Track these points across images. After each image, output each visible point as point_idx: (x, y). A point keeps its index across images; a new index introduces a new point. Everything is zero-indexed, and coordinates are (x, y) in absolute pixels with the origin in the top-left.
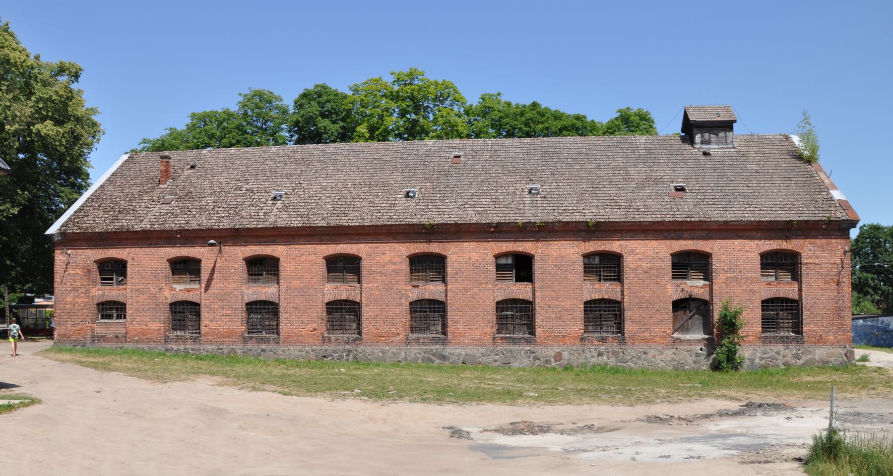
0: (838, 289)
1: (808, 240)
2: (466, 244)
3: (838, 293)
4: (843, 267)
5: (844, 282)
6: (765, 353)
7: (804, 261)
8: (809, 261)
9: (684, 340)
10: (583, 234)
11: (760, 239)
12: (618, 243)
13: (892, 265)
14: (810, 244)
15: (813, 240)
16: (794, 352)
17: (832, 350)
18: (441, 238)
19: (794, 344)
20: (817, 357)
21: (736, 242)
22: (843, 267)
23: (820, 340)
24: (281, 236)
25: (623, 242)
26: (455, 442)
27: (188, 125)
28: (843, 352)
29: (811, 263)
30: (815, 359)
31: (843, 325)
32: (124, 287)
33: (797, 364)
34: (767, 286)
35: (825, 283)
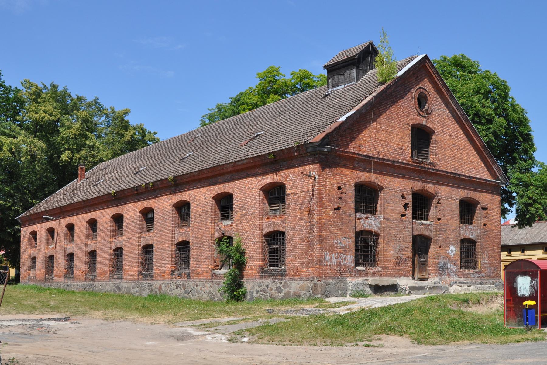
0: (309, 219)
1: (290, 170)
2: (130, 205)
3: (310, 222)
4: (313, 195)
5: (314, 210)
6: (260, 286)
7: (288, 191)
8: (291, 191)
9: (218, 274)
10: (173, 189)
11: (260, 175)
12: (188, 193)
13: (1, 263)
14: (292, 173)
15: (294, 169)
16: (278, 285)
17: (303, 283)
18: (68, 214)
19: (280, 277)
20: (292, 291)
21: (247, 180)
22: (313, 195)
23: (297, 274)
24: (74, 210)
25: (190, 191)
26: (223, 333)
27: (137, 125)
28: (310, 285)
29: (292, 193)
30: (290, 292)
31: (313, 256)
32: (96, 233)
33: (279, 297)
34: (267, 220)
35: (301, 213)
